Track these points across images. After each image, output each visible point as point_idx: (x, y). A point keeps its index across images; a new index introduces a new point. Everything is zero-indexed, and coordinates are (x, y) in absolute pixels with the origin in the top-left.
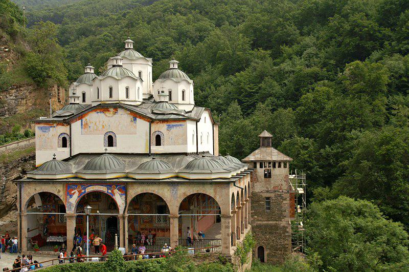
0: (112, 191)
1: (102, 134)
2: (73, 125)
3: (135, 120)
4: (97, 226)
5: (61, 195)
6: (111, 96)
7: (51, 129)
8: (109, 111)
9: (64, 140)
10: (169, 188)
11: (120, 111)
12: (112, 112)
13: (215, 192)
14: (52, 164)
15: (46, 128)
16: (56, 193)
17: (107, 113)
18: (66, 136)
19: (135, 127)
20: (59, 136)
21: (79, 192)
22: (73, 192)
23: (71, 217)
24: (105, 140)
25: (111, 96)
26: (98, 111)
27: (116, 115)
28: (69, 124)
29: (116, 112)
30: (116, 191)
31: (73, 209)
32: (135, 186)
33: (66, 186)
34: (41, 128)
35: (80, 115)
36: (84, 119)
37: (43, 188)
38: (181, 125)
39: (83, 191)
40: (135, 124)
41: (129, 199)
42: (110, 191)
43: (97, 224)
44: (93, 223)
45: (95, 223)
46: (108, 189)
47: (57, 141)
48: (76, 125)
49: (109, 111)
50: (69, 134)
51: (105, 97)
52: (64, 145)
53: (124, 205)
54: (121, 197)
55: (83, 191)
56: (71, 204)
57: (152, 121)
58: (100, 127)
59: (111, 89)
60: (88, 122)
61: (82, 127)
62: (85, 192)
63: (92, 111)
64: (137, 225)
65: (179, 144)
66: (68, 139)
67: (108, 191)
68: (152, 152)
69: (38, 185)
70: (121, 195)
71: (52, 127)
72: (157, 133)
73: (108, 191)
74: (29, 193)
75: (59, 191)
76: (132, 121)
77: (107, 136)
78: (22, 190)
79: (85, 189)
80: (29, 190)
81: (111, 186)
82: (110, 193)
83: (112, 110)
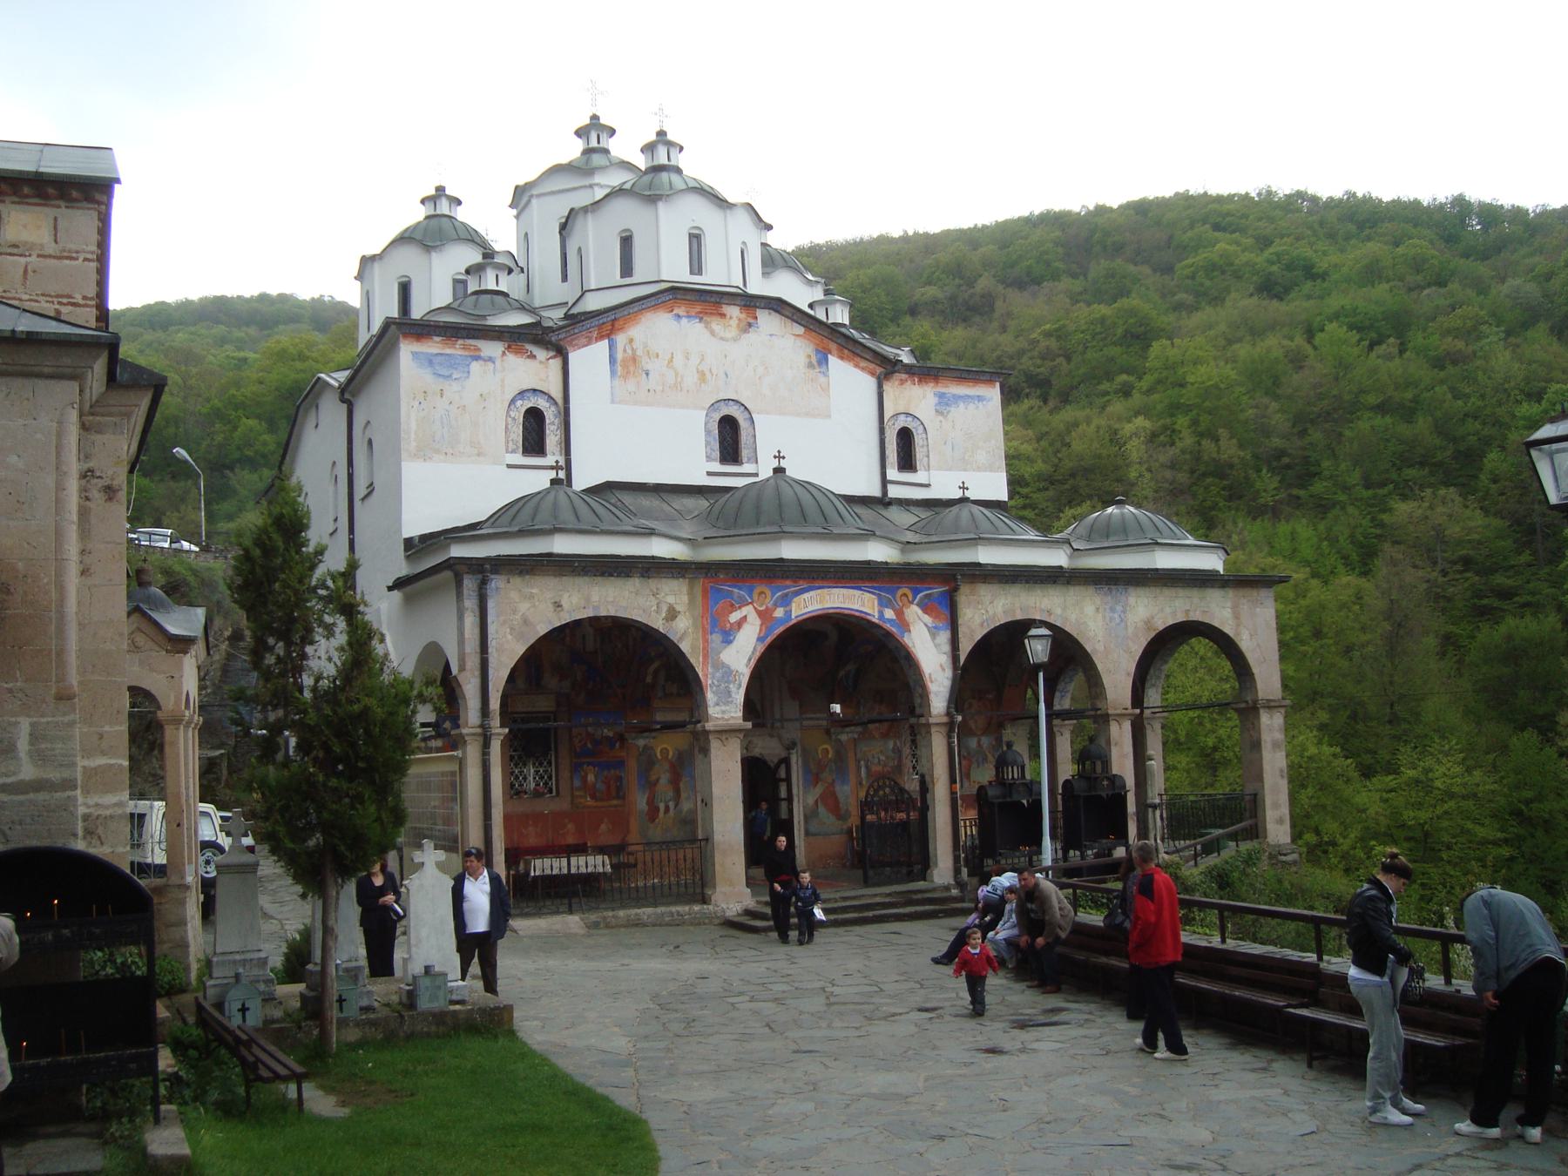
0: (900, 614)
1: (703, 408)
2: (574, 357)
3: (823, 361)
4: (686, 806)
5: (684, 632)
6: (696, 266)
7: (475, 367)
8: (723, 315)
9: (534, 419)
10: (1098, 600)
11: (768, 321)
12: (734, 322)
13: (1237, 616)
14: (555, 505)
15: (451, 362)
16: (658, 623)
17: (716, 324)
18: (542, 404)
19: (826, 389)
20: (513, 401)
21: (764, 616)
22: (734, 617)
23: (726, 732)
24: (708, 432)
25: (696, 266)
26: (681, 311)
27: (752, 336)
28: (561, 353)
29: (750, 325)
30: (914, 612)
31: (739, 696)
32: (985, 592)
33: (705, 592)
34: (430, 361)
35: (606, 323)
36: (621, 339)
37: (595, 598)
38: (980, 398)
39: (779, 613)
40: (822, 379)
41: (966, 647)
42: (889, 614)
43: (684, 795)
44: (671, 794)
45: (677, 792)
46: (883, 604)
47: (504, 428)
48: (589, 360)
49: (723, 315)
50: (557, 394)
51: (676, 270)
52: (534, 442)
53: (949, 673)
54: (933, 636)
55: (779, 613)
56: (729, 674)
57: (886, 368)
58: (691, 379)
59: (695, 239)
60: (639, 353)
61: (613, 372)
62: (788, 613)
63: (655, 307)
64: (847, 788)
65: (979, 469)
66: (550, 415)
67: (881, 614)
68: (894, 492)
69: (568, 581)
70: (933, 632)
71: (477, 358)
72: (902, 422)
73: (881, 614)
74: (526, 622)
75: (672, 614)
76: (810, 365)
77: (717, 416)
78: (491, 604)
79: (785, 601)
80: (524, 607)
81: (893, 592)
82: (890, 621)
83: (734, 312)
